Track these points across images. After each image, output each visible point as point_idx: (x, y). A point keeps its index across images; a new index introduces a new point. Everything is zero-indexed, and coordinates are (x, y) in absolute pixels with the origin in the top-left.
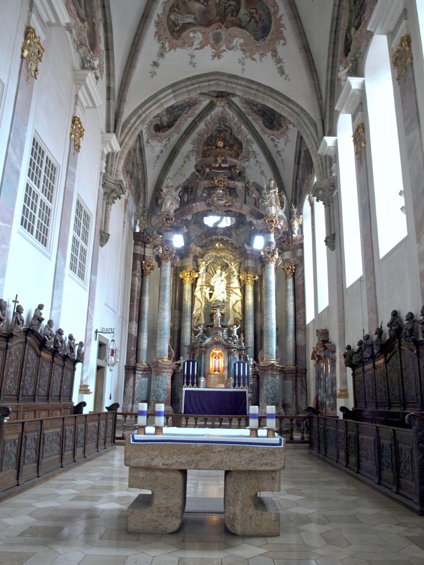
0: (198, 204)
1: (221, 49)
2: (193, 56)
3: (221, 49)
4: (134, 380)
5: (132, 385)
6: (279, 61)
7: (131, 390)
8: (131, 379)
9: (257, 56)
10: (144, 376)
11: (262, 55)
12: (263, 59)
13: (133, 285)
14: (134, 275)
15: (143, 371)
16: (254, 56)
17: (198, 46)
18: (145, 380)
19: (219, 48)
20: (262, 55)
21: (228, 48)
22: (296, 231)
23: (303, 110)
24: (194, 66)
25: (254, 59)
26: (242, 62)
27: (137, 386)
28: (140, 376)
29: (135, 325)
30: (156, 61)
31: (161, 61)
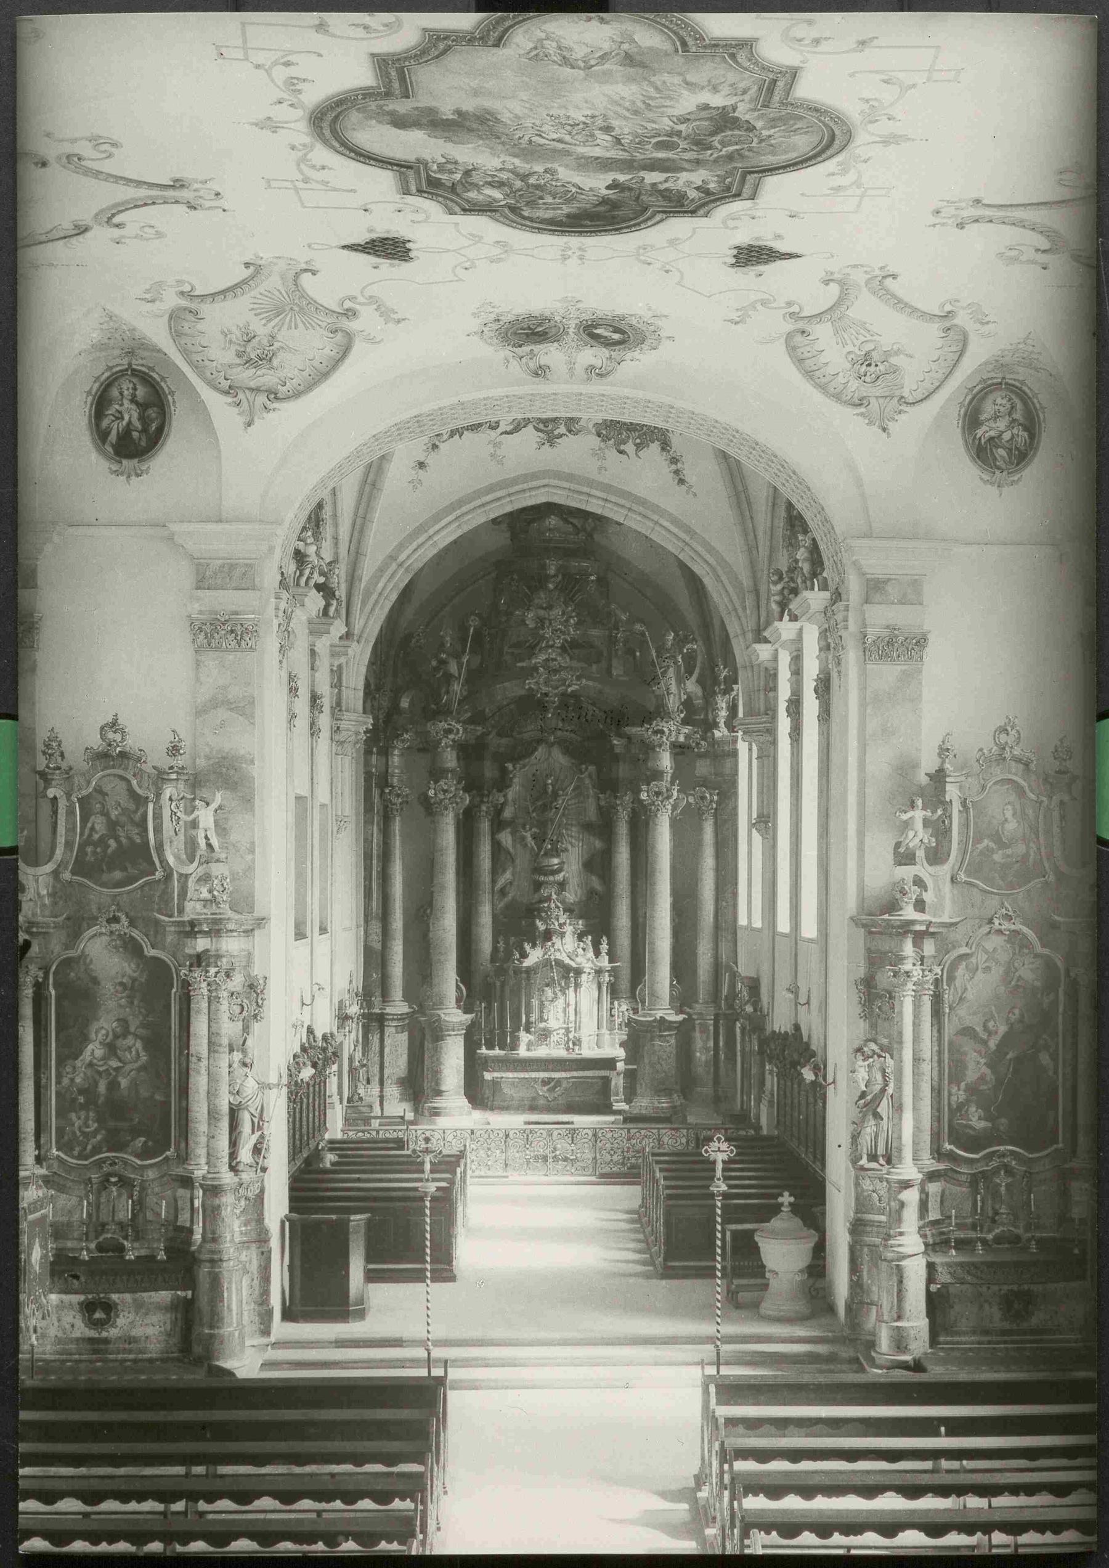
0: (507, 684)
1: (556, 433)
2: (497, 445)
3: (556, 433)
4: (382, 1040)
5: (377, 1049)
6: (674, 461)
7: (377, 1059)
8: (375, 1039)
9: (629, 447)
10: (400, 1030)
11: (639, 447)
12: (641, 453)
13: (368, 842)
14: (368, 822)
15: (398, 1020)
16: (622, 447)
17: (509, 428)
18: (404, 1037)
19: (552, 431)
20: (639, 447)
21: (570, 431)
22: (722, 722)
23: (722, 561)
24: (500, 462)
25: (621, 452)
26: (596, 454)
27: (387, 1050)
28: (393, 1030)
29: (376, 927)
30: (422, 460)
31: (431, 460)
